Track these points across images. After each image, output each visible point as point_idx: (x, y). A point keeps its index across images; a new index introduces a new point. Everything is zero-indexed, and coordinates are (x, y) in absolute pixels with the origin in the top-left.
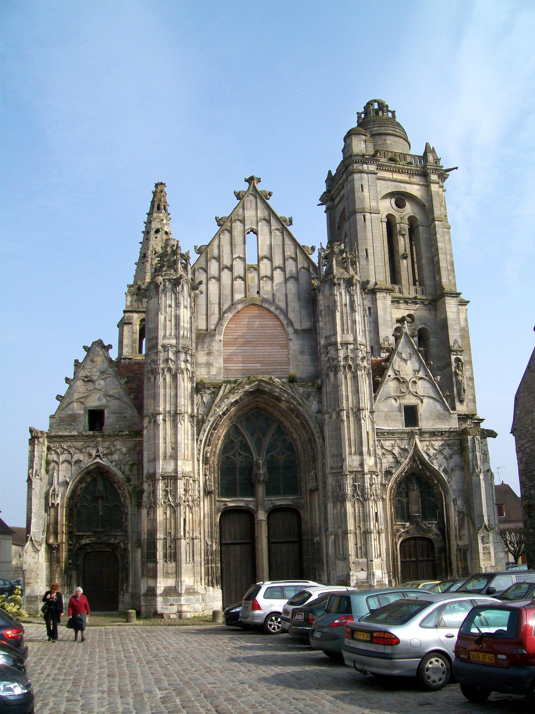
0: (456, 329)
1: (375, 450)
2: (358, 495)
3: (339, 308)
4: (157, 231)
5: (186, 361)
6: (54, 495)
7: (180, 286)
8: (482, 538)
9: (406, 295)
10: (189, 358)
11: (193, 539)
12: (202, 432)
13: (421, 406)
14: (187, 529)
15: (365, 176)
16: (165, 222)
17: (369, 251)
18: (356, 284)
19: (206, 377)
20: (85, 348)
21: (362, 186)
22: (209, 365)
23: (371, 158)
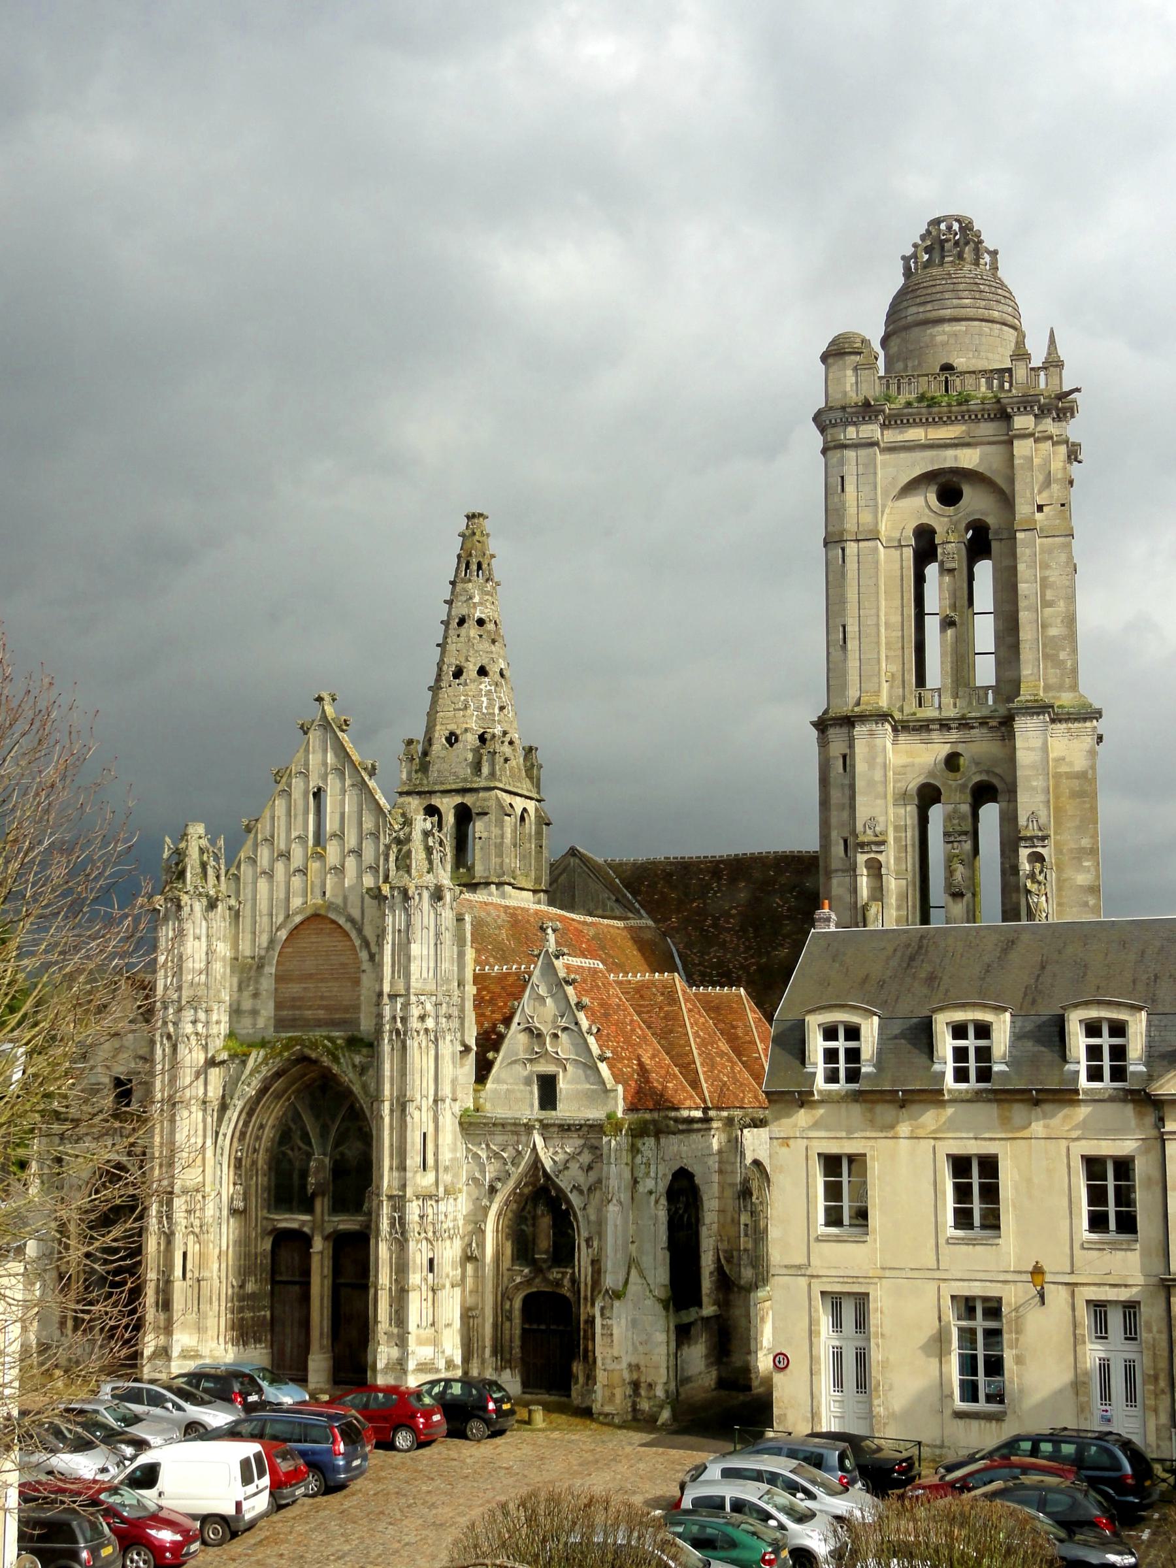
0: (1034, 789)
3: (389, 938)
4: (462, 622)
5: (194, 1022)
8: (602, 1309)
10: (202, 1015)
11: (199, 1281)
13: (564, 1077)
14: (189, 1266)
15: (850, 454)
16: (476, 599)
17: (848, 629)
19: (251, 1031)
21: (842, 477)
22: (255, 1013)
23: (861, 409)
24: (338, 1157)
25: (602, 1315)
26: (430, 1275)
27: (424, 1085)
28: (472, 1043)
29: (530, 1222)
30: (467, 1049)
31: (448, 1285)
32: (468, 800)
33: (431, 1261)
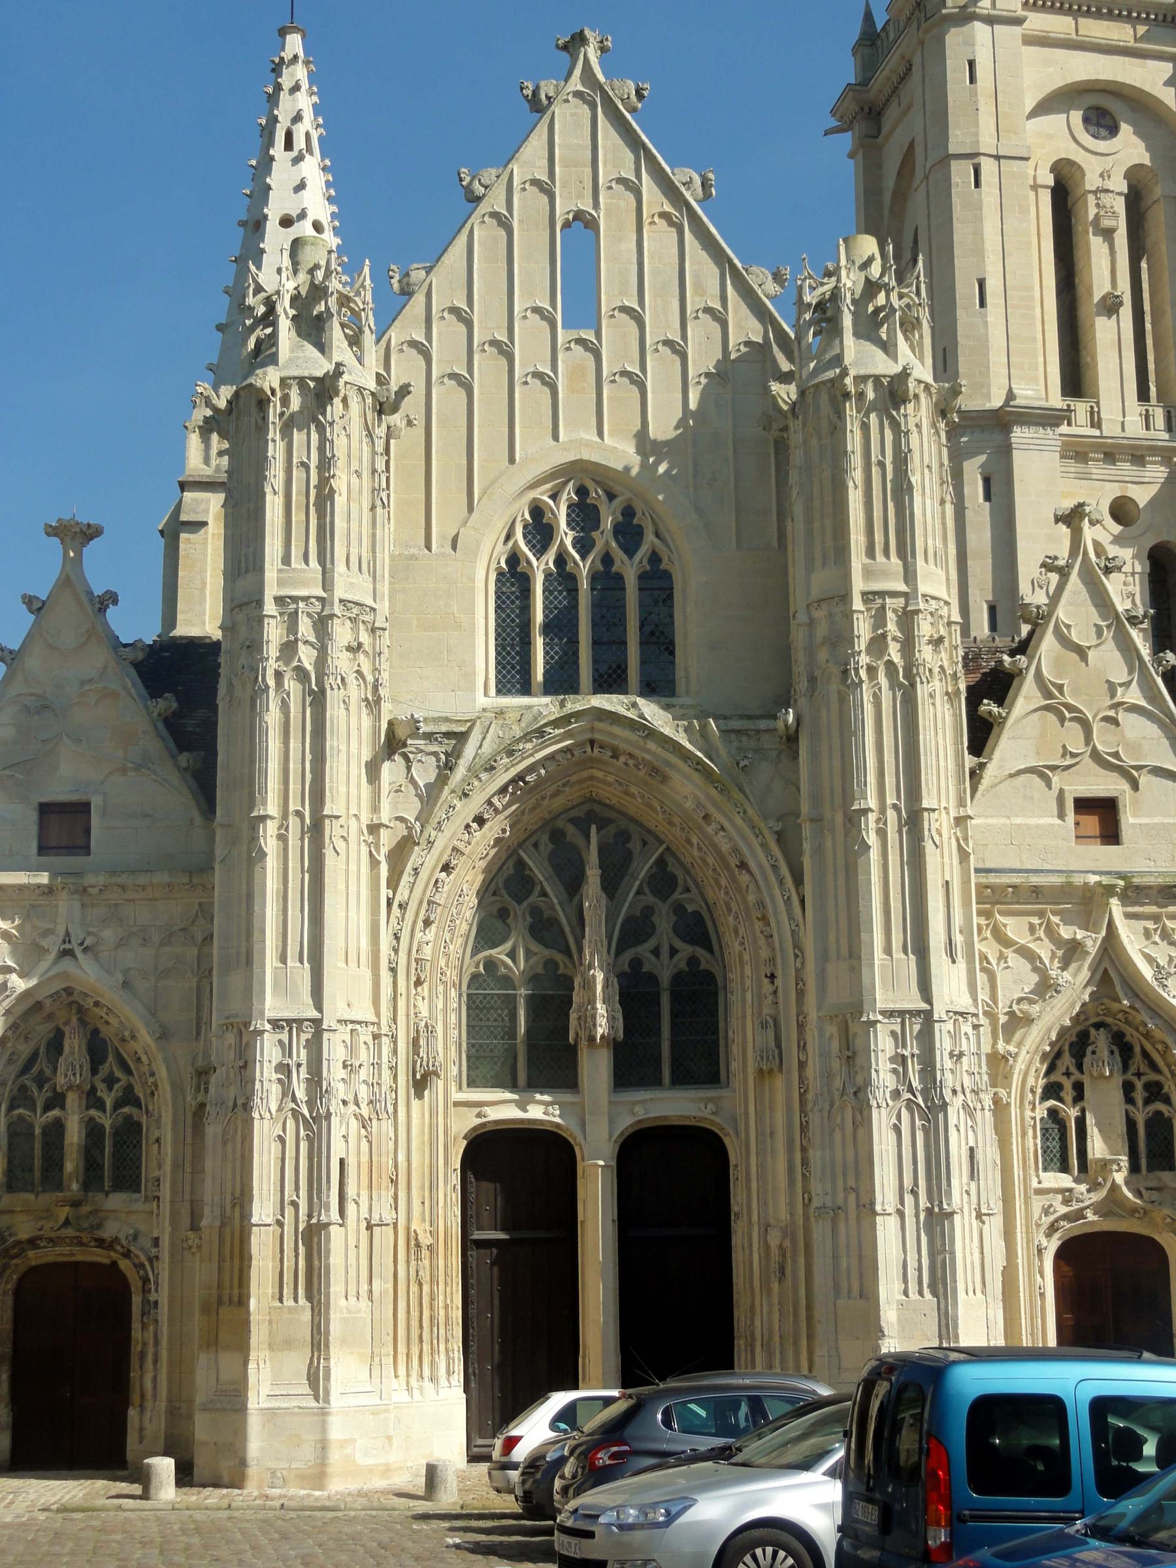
1: (969, 945)
2: (910, 1089)
5: (355, 649)
7: (337, 401)
9: (1110, 429)
10: (364, 637)
12: (406, 879)
13: (1135, 802)
14: (351, 1191)
18: (916, 396)
20: (29, 601)
21: (971, 64)
26: (973, 1185)
29: (1068, 1093)
33: (971, 1149)
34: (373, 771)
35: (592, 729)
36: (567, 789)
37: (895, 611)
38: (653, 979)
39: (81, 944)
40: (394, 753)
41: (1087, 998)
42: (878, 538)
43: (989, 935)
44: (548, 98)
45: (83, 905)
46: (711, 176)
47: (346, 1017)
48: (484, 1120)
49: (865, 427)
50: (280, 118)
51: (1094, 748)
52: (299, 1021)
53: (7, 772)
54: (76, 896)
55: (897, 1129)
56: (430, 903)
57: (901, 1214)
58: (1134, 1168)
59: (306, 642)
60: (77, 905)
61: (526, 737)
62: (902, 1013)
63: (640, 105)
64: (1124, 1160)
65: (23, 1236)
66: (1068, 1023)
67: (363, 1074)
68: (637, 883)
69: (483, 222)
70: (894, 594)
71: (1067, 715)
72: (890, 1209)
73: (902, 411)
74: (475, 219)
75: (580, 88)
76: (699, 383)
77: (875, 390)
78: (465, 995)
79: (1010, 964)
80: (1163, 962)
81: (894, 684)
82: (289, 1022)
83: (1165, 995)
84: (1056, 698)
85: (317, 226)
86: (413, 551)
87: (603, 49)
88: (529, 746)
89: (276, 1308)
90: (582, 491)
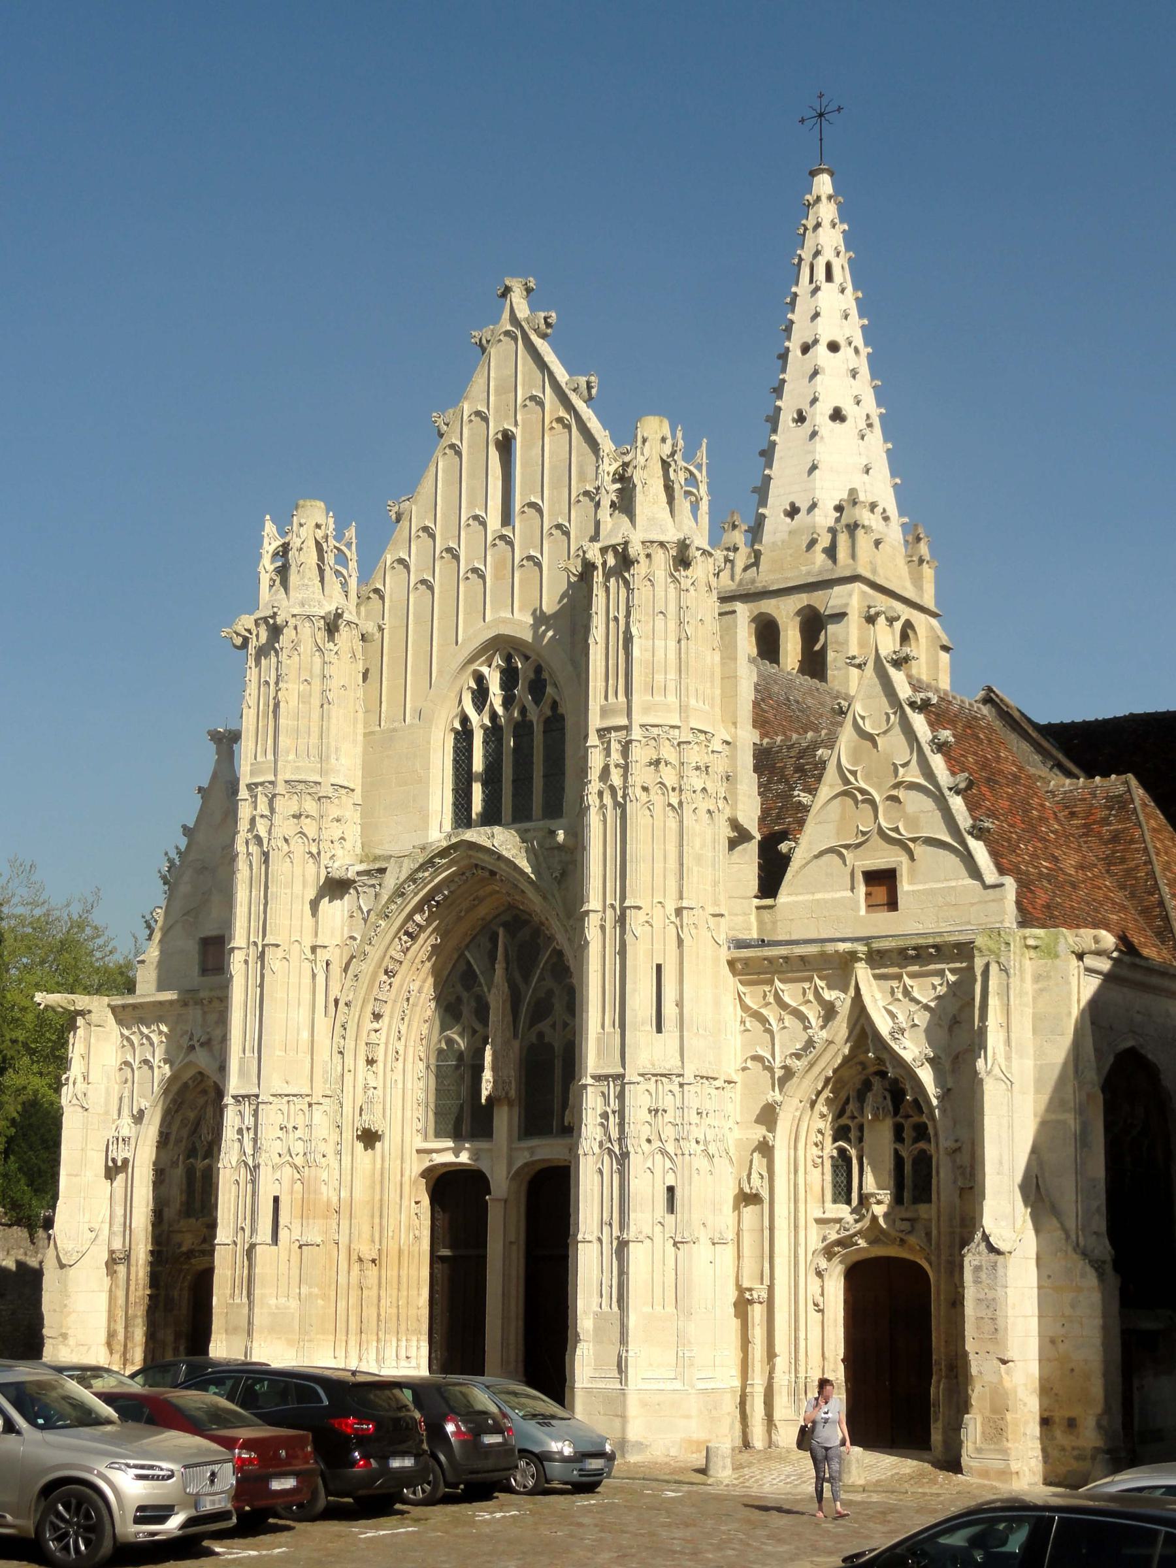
2: (610, 1141)
6: (117, 1139)
10: (310, 806)
13: (912, 873)
14: (283, 1221)
20: (200, 789)
24: (534, 1040)
25: (977, 1282)
26: (670, 1219)
27: (658, 880)
28: (753, 828)
30: (739, 837)
31: (704, 1241)
32: (816, 599)
33: (671, 1190)
34: (315, 905)
35: (470, 857)
36: (476, 902)
37: (620, 742)
38: (550, 1047)
39: (198, 1041)
40: (349, 888)
41: (846, 1051)
42: (610, 682)
43: (771, 1000)
44: (488, 342)
45: (204, 1013)
46: (593, 379)
47: (280, 1092)
48: (432, 1163)
49: (607, 589)
50: (803, 256)
51: (880, 827)
52: (248, 1096)
53: (185, 917)
54: (198, 1007)
55: (601, 1172)
56: (375, 999)
57: (600, 1240)
58: (898, 1199)
59: (262, 816)
60: (199, 1012)
61: (422, 867)
62: (606, 1077)
63: (549, 331)
64: (886, 1196)
65: (184, 1249)
66: (830, 1074)
67: (298, 1134)
68: (539, 971)
69: (445, 454)
70: (617, 729)
71: (860, 797)
72: (593, 1238)
73: (632, 572)
74: (438, 453)
75: (509, 327)
76: (578, 556)
77: (615, 557)
78: (433, 1068)
79: (787, 1024)
80: (902, 1018)
81: (616, 804)
82: (243, 1097)
83: (896, 1047)
84: (851, 784)
85: (834, 347)
86: (396, 724)
87: (529, 291)
88: (426, 874)
89: (230, 1304)
90: (508, 659)
